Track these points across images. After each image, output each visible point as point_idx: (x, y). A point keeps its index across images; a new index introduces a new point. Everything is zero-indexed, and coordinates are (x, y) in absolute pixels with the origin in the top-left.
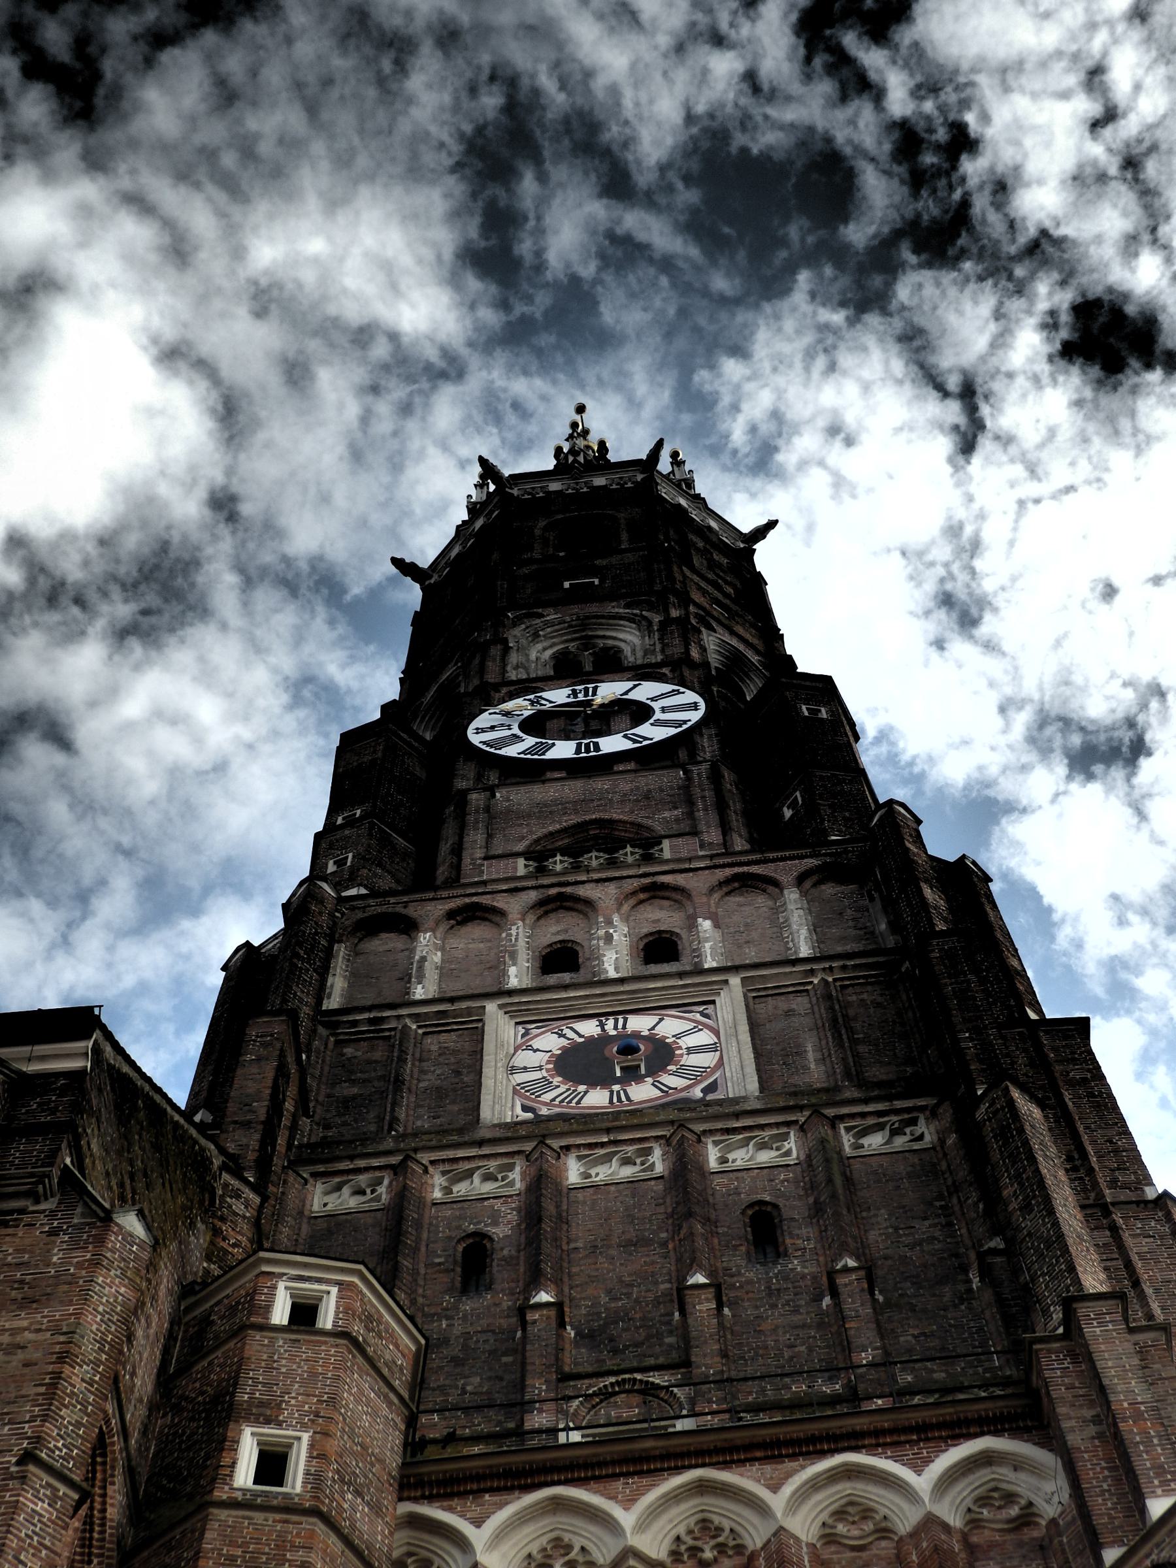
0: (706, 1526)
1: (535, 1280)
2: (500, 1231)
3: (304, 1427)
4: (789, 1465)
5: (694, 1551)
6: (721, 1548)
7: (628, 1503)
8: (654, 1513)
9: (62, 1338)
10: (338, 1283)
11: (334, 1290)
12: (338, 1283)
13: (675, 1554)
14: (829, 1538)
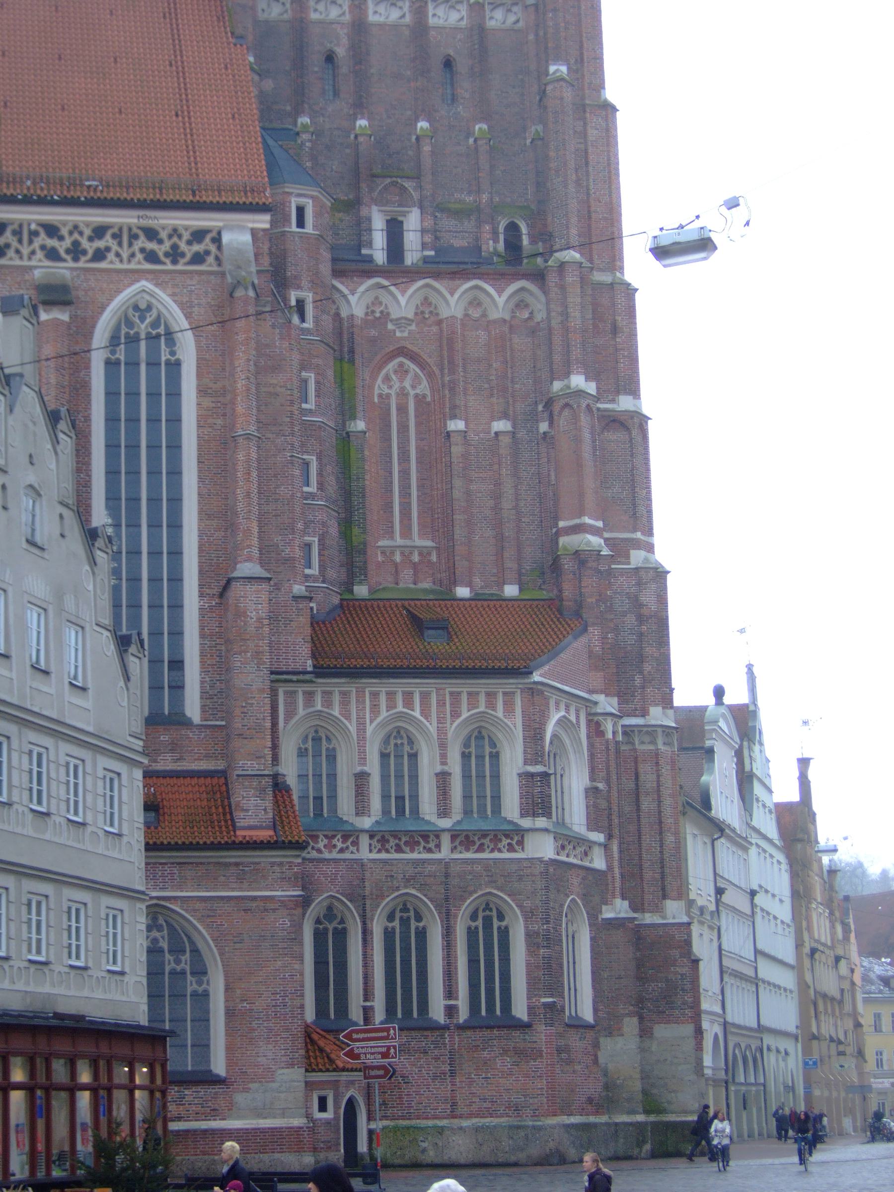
0: (426, 301)
1: (359, 106)
2: (341, 52)
3: (310, 290)
4: (458, 282)
5: (423, 312)
6: (431, 312)
7: (403, 292)
8: (411, 296)
9: (289, 392)
10: (312, 197)
11: (310, 201)
12: (312, 197)
13: (416, 314)
14: (466, 315)
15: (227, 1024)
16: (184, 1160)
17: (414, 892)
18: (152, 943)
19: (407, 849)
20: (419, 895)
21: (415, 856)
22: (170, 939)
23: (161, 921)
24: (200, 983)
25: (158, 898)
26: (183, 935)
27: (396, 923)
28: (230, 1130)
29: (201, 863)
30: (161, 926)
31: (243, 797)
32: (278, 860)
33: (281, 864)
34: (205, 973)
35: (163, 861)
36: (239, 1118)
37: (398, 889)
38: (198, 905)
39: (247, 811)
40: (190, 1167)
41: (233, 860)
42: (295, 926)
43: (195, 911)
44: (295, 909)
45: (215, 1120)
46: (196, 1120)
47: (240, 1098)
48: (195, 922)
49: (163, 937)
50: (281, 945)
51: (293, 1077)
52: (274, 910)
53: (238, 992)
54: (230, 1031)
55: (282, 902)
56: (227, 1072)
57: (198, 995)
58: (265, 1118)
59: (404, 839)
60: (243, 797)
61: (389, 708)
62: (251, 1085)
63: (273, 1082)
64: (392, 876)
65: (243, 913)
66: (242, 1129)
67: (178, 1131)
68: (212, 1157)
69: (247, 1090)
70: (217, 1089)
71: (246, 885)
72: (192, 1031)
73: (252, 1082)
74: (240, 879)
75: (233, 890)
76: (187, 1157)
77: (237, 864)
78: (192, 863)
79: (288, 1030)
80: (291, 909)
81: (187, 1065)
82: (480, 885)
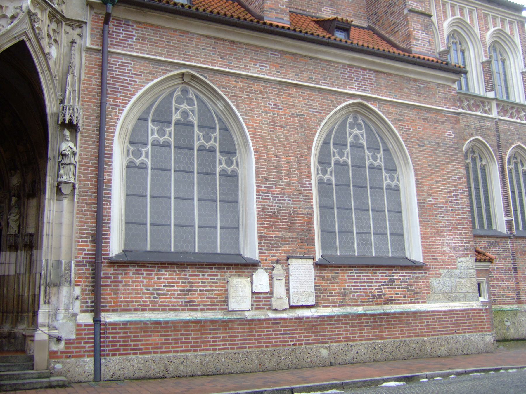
15: (420, 216)
16: (401, 341)
17: (481, 138)
18: (354, 139)
19: (474, 109)
20: (484, 141)
21: (478, 113)
22: (367, 137)
23: (360, 121)
24: (392, 179)
25: (362, 97)
26: (377, 135)
27: (469, 161)
28: (433, 312)
29: (391, 74)
30: (360, 125)
31: (415, 29)
32: (441, 82)
33: (443, 86)
34: (395, 170)
35: (364, 66)
36: (437, 301)
37: (472, 135)
38: (391, 110)
39: (418, 40)
40: (407, 349)
41: (412, 76)
42: (457, 137)
43: (390, 113)
44: (456, 124)
45: (418, 303)
46: (405, 303)
47: (435, 282)
48: (390, 123)
49: (362, 135)
50: (450, 152)
51: (467, 263)
52: (443, 123)
53: (426, 187)
54: (423, 222)
55: (447, 117)
56: (424, 259)
57: (391, 189)
58: (453, 301)
59: (472, 102)
60: (415, 29)
61: (453, 16)
62: (441, 271)
63: (456, 268)
64: (468, 126)
65: (422, 121)
66: (441, 311)
67: (394, 313)
68: (422, 338)
69: (439, 275)
70: (417, 274)
71: (422, 99)
72: (389, 221)
73: (440, 268)
74: (418, 93)
75: (414, 100)
76: (403, 339)
77: (415, 80)
78: (384, 73)
79: (461, 224)
80: (453, 123)
81: (372, 252)
82: (515, 139)
